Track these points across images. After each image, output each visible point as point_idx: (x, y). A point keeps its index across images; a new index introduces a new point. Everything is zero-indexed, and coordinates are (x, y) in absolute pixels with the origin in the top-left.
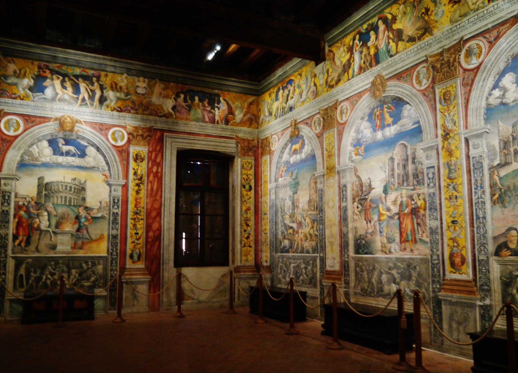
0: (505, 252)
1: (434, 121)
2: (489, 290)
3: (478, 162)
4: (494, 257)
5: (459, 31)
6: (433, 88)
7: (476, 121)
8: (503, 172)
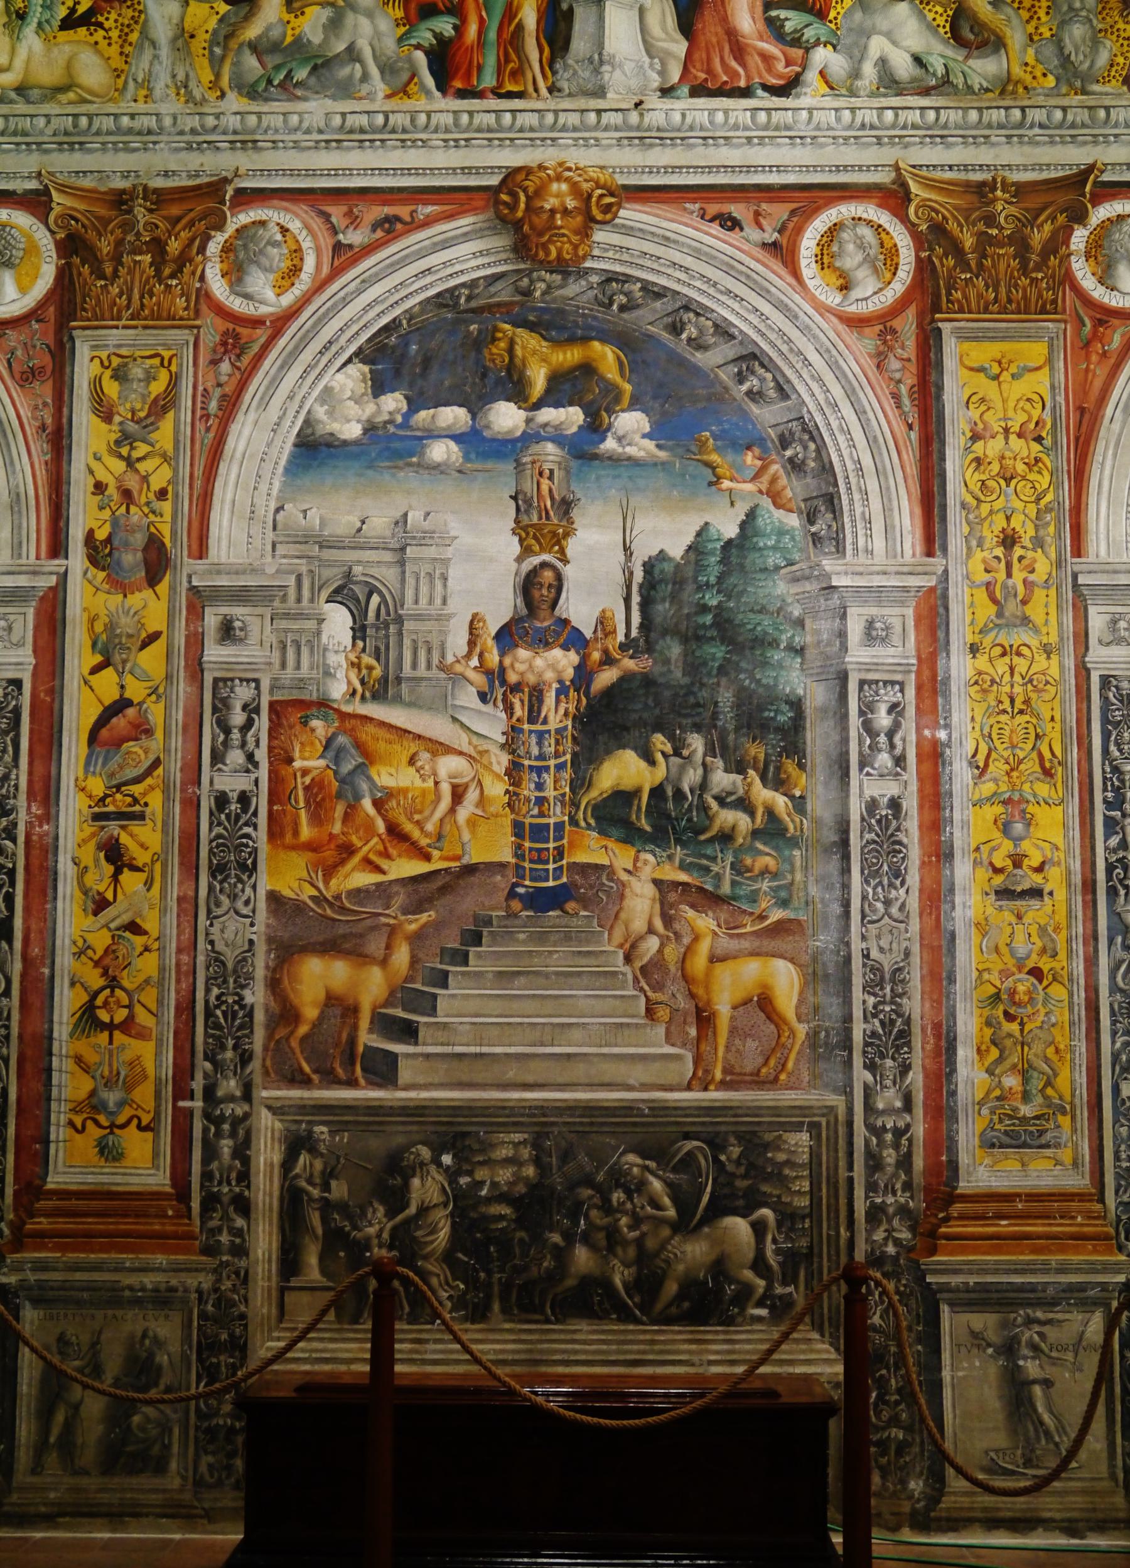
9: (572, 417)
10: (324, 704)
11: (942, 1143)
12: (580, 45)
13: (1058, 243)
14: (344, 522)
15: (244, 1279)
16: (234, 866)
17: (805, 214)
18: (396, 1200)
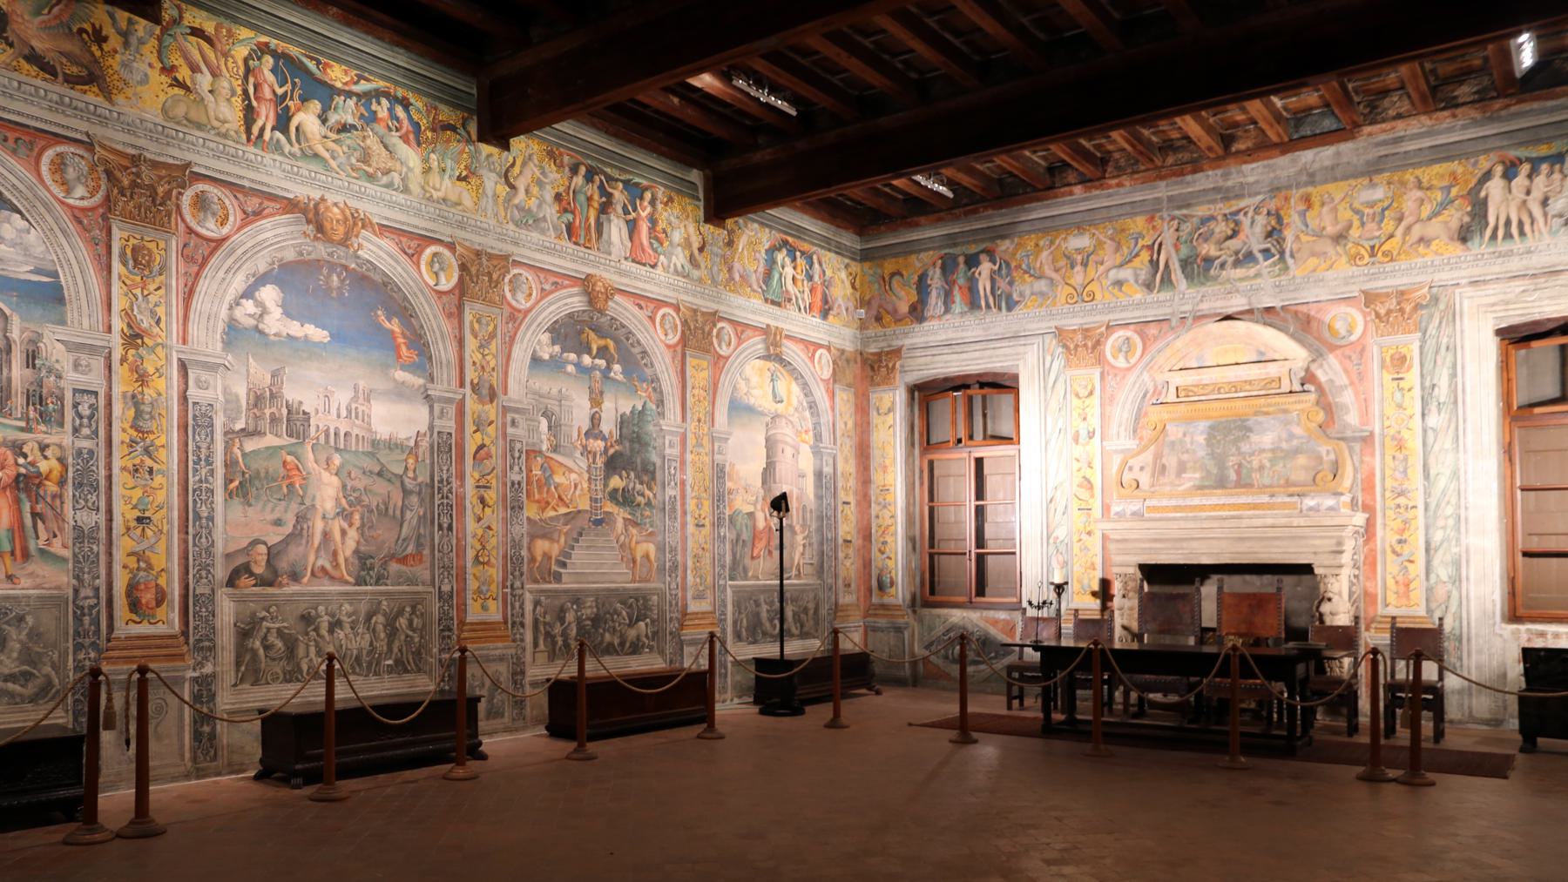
0: (245, 581)
1: (104, 292)
2: (212, 649)
3: (204, 415)
4: (225, 589)
5: (184, 145)
6: (105, 218)
7: (206, 339)
8: (251, 445)
9: (602, 363)
10: (540, 452)
11: (684, 598)
12: (605, 236)
13: (710, 333)
14: (545, 389)
15: (524, 649)
16: (517, 507)
17: (658, 308)
18: (562, 620)
